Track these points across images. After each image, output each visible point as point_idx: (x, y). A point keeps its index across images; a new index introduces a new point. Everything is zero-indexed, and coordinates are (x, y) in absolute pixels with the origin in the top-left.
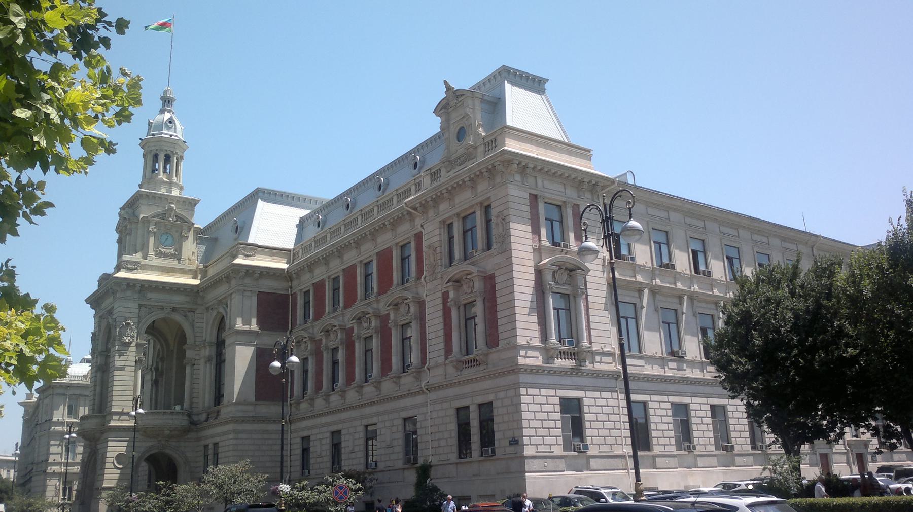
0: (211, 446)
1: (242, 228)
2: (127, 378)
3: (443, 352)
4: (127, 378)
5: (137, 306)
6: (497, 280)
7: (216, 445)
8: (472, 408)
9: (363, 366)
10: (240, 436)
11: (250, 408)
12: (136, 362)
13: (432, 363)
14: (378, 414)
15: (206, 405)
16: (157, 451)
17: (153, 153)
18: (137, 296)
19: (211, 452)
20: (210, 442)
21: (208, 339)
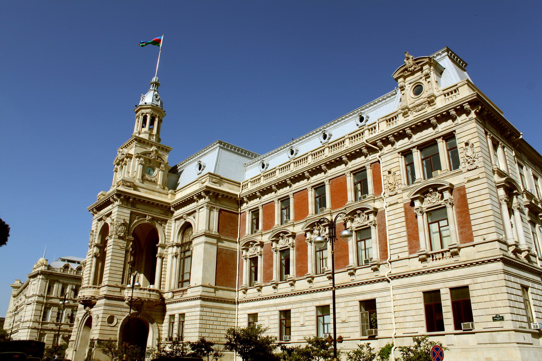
0: (177, 316)
1: (204, 167)
2: (120, 262)
3: (406, 249)
4: (120, 262)
5: (129, 212)
6: (467, 191)
7: (182, 315)
8: (442, 292)
9: (314, 262)
10: (205, 309)
13: (394, 258)
14: (259, 307)
15: (172, 286)
17: (144, 115)
19: (176, 319)
20: (177, 313)
21: (176, 241)
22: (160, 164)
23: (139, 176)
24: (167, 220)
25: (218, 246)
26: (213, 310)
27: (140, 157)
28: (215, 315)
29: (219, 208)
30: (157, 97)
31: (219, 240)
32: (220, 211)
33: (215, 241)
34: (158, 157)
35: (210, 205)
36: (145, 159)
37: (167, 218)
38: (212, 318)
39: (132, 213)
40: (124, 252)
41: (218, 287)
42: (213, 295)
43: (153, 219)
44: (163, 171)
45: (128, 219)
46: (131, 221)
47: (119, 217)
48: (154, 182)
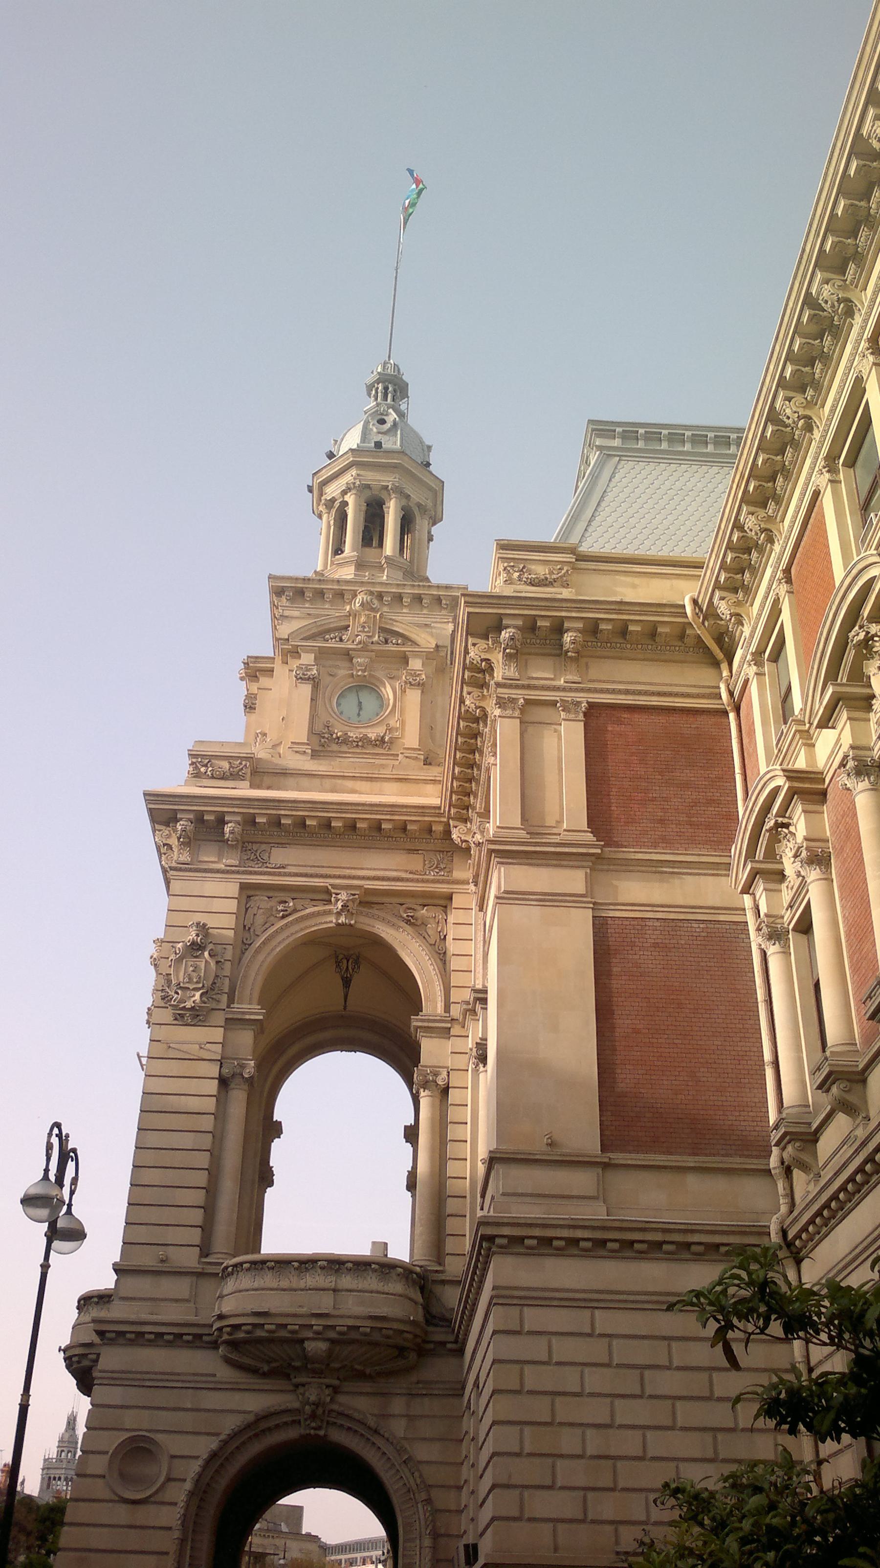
4: (188, 1140)
11: (581, 1181)
12: (224, 1082)
16: (292, 1434)
18: (231, 860)
22: (404, 659)
23: (300, 732)
24: (450, 898)
25: (596, 906)
26: (605, 1321)
27: (295, 653)
28: (622, 1352)
29: (584, 698)
30: (382, 422)
31: (596, 864)
32: (594, 715)
33: (573, 880)
34: (388, 633)
35: (520, 695)
36: (322, 655)
37: (444, 888)
38: (595, 1380)
39: (248, 891)
40: (212, 1087)
41: (618, 1157)
42: (597, 1212)
43: (369, 901)
44: (421, 685)
45: (230, 921)
46: (245, 930)
47: (179, 919)
48: (381, 742)
